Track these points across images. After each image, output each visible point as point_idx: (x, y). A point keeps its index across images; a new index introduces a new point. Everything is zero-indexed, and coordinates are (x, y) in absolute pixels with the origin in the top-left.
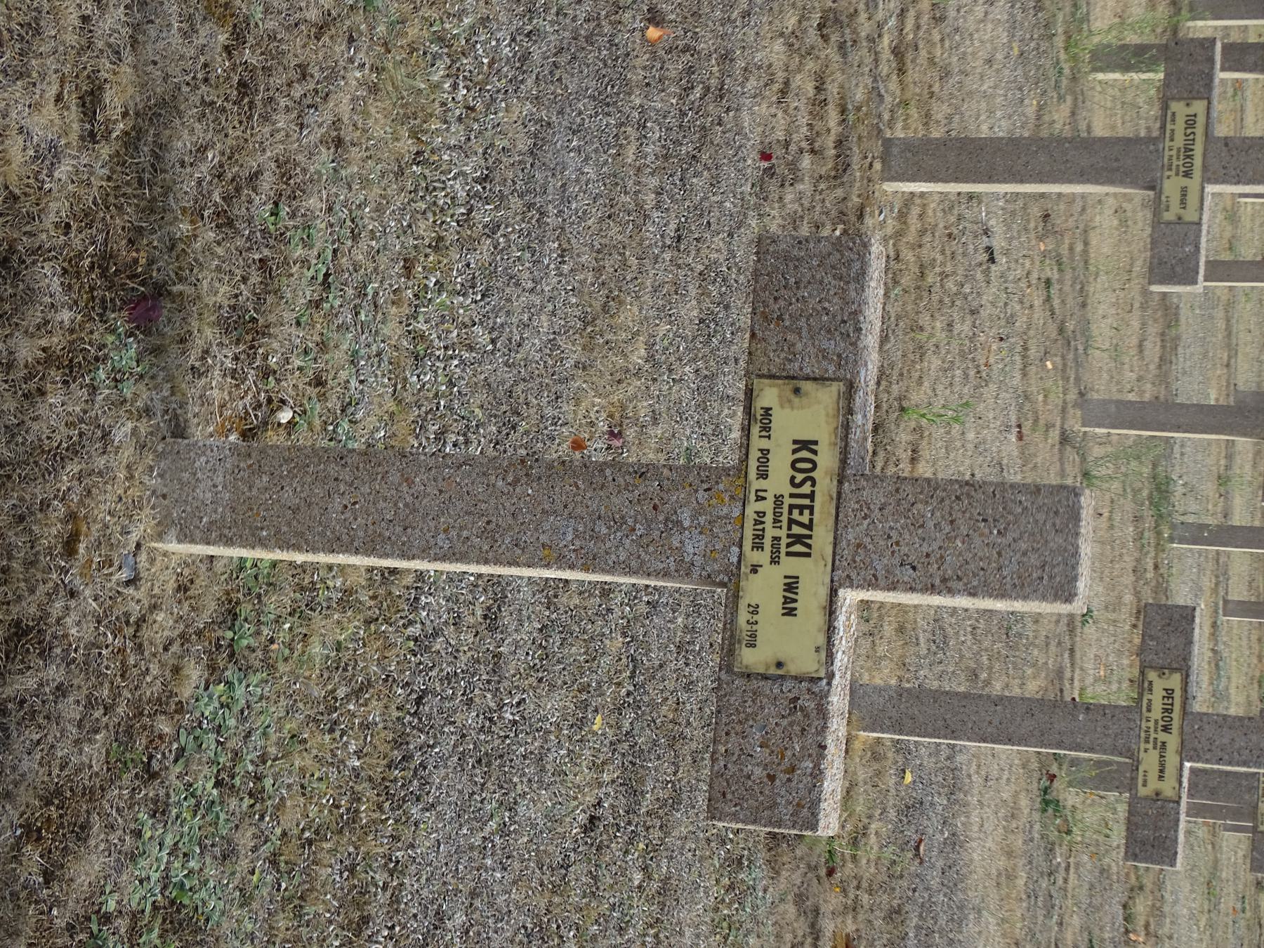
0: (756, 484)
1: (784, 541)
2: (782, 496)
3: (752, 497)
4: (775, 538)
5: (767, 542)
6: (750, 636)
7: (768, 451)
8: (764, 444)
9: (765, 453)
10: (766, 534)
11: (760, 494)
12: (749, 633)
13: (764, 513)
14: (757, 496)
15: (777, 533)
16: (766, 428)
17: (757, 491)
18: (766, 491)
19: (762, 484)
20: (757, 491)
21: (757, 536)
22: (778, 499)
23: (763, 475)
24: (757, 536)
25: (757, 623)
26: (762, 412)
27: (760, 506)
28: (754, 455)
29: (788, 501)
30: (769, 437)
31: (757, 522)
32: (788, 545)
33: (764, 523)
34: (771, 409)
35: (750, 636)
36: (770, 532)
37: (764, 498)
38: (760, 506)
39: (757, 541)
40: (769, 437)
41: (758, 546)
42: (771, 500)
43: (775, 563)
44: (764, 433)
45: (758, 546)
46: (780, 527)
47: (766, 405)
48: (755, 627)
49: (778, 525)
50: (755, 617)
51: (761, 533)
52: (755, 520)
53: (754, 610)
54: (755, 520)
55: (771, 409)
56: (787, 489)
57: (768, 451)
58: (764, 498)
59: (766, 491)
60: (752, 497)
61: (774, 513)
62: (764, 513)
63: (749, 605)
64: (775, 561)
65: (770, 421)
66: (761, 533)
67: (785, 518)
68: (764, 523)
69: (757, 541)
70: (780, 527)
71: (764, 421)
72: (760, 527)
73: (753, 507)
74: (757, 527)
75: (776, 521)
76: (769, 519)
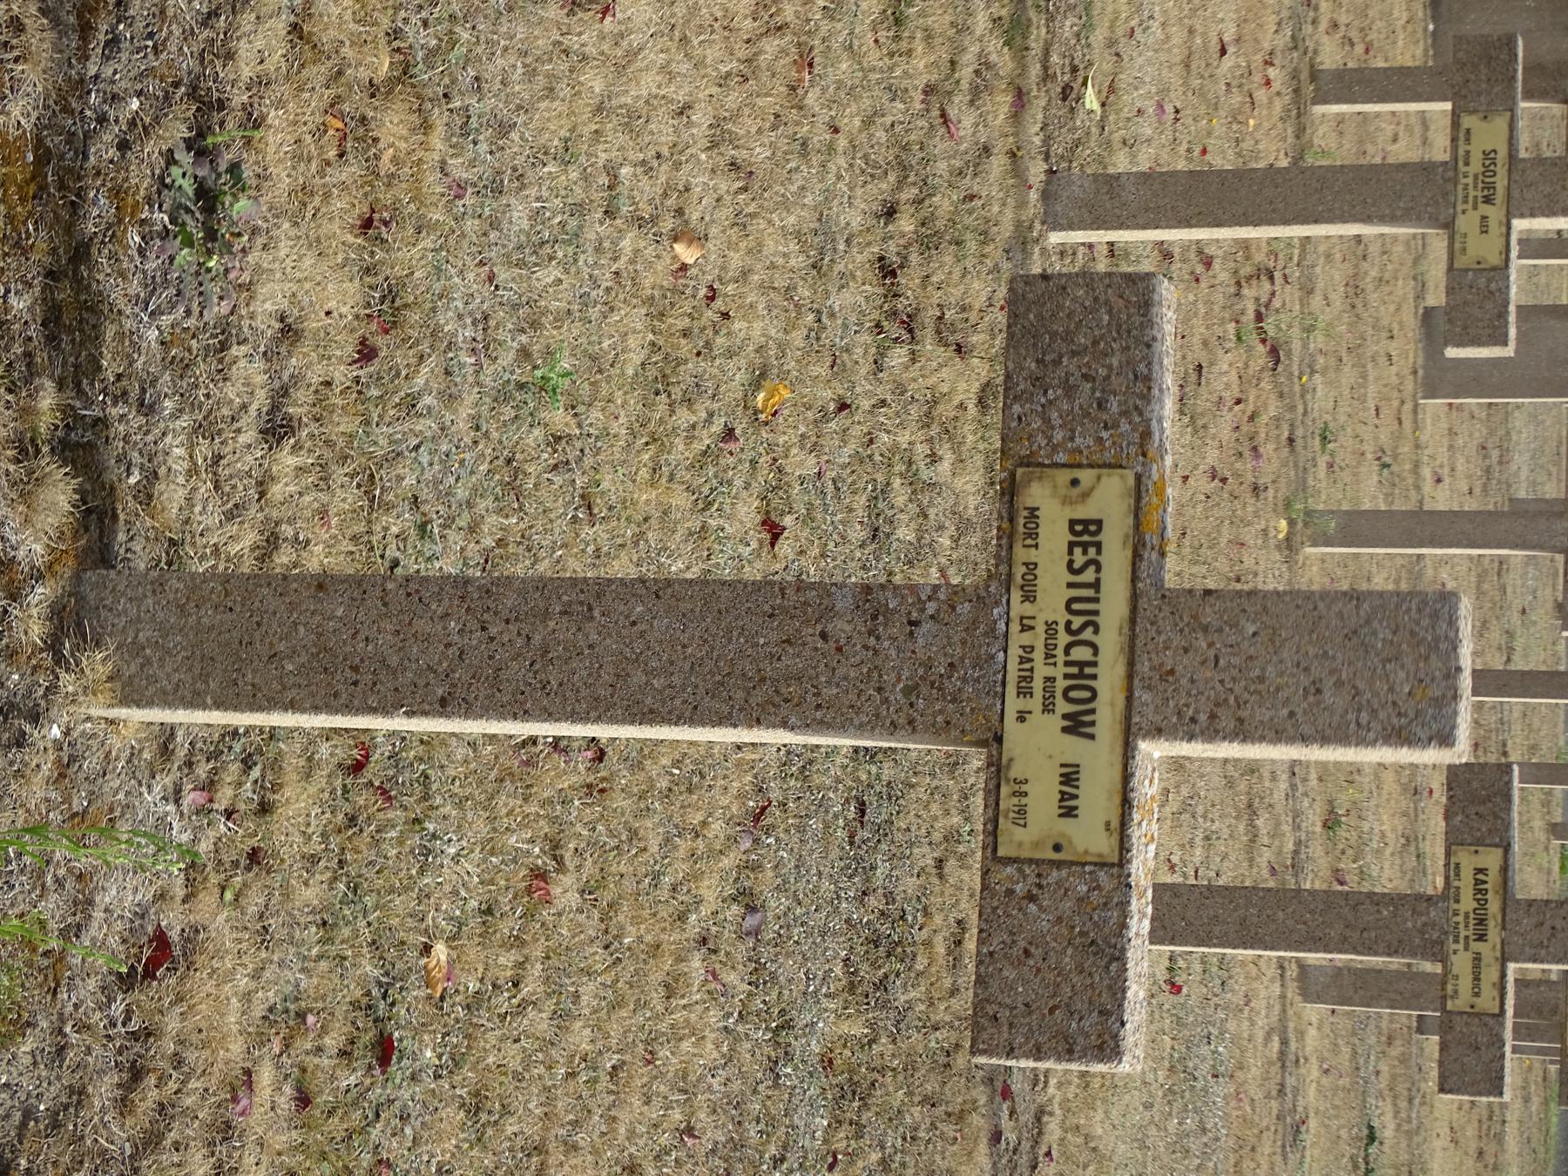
0: (1018, 607)
1: (1061, 684)
3: (1015, 627)
4: (1047, 679)
5: (1038, 685)
6: (1018, 813)
7: (1036, 564)
10: (1035, 676)
11: (1025, 621)
12: (1016, 809)
13: (1032, 648)
14: (1022, 625)
15: (1050, 672)
17: (1022, 618)
18: (1034, 618)
19: (1028, 609)
20: (1022, 618)
22: (1051, 627)
24: (1024, 678)
25: (1026, 794)
27: (1026, 639)
28: (1019, 571)
30: (1036, 546)
31: (1022, 660)
33: (1031, 660)
34: (1038, 509)
35: (1018, 813)
36: (1041, 671)
37: (1032, 628)
38: (1026, 639)
39: (1023, 684)
40: (1036, 546)
42: (1041, 629)
43: (1049, 711)
44: (1029, 542)
46: (1055, 664)
47: (1036, 505)
48: (1024, 801)
49: (1052, 661)
50: (1024, 788)
51: (1028, 674)
52: (1020, 657)
54: (1020, 657)
55: (1038, 509)
56: (1062, 617)
57: (1036, 564)
58: (1032, 628)
59: (1034, 618)
60: (1015, 627)
61: (1046, 645)
64: (1048, 708)
65: (1038, 526)
66: (1028, 674)
67: (1060, 652)
68: (1032, 660)
69: (1023, 684)
70: (1055, 664)
71: (1033, 526)
72: (1027, 666)
73: (1017, 639)
74: (1027, 666)
75: (1048, 656)
76: (1038, 655)
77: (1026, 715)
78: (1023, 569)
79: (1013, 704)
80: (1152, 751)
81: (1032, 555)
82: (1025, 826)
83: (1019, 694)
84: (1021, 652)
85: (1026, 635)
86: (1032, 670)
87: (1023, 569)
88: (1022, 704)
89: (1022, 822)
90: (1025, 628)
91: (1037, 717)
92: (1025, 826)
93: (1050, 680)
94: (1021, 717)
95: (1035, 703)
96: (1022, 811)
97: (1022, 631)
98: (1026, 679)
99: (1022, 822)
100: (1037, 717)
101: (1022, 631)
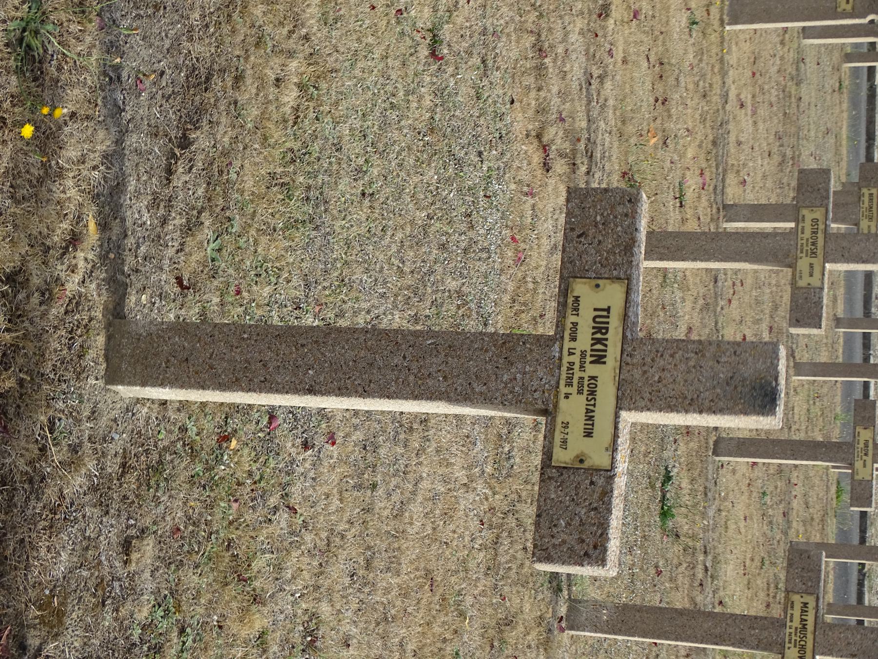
0: (567, 344)
2: (586, 351)
5: (575, 381)
7: (577, 323)
8: (573, 319)
9: (575, 324)
10: (574, 377)
13: (574, 363)
14: (569, 352)
15: (582, 374)
16: (576, 309)
17: (569, 349)
19: (572, 345)
21: (568, 378)
23: (573, 339)
24: (568, 378)
25: (567, 434)
26: (573, 299)
27: (572, 359)
29: (589, 353)
30: (578, 315)
31: (569, 369)
32: (589, 380)
33: (573, 369)
34: (579, 297)
36: (577, 374)
37: (574, 354)
38: (572, 359)
40: (578, 315)
41: (569, 384)
42: (578, 353)
44: (574, 312)
45: (569, 384)
46: (584, 371)
48: (566, 436)
50: (567, 431)
53: (566, 425)
55: (579, 297)
57: (577, 323)
58: (574, 354)
62: (574, 363)
63: (563, 423)
64: (580, 392)
68: (573, 369)
72: (571, 372)
73: (566, 359)
75: (581, 367)
77: (570, 396)
78: (572, 326)
79: (563, 389)
80: (628, 417)
81: (573, 319)
82: (566, 449)
83: (566, 385)
84: (568, 365)
85: (572, 357)
86: (573, 374)
87: (572, 326)
88: (569, 390)
89: (564, 447)
90: (570, 354)
91: (575, 397)
92: (566, 449)
93: (582, 378)
94: (567, 397)
95: (574, 390)
96: (564, 442)
97: (569, 355)
98: (570, 378)
99: (564, 447)
100: (575, 397)
101: (569, 355)
